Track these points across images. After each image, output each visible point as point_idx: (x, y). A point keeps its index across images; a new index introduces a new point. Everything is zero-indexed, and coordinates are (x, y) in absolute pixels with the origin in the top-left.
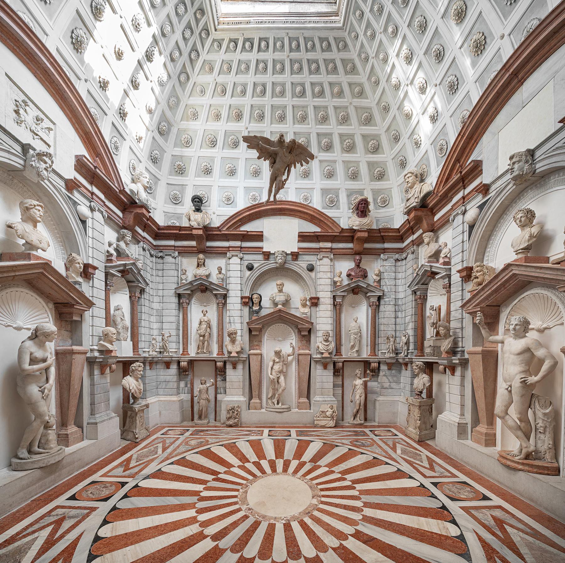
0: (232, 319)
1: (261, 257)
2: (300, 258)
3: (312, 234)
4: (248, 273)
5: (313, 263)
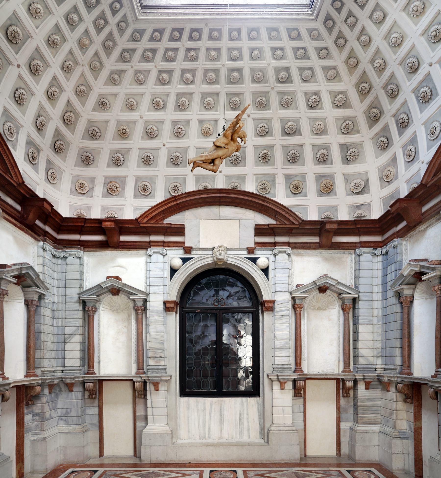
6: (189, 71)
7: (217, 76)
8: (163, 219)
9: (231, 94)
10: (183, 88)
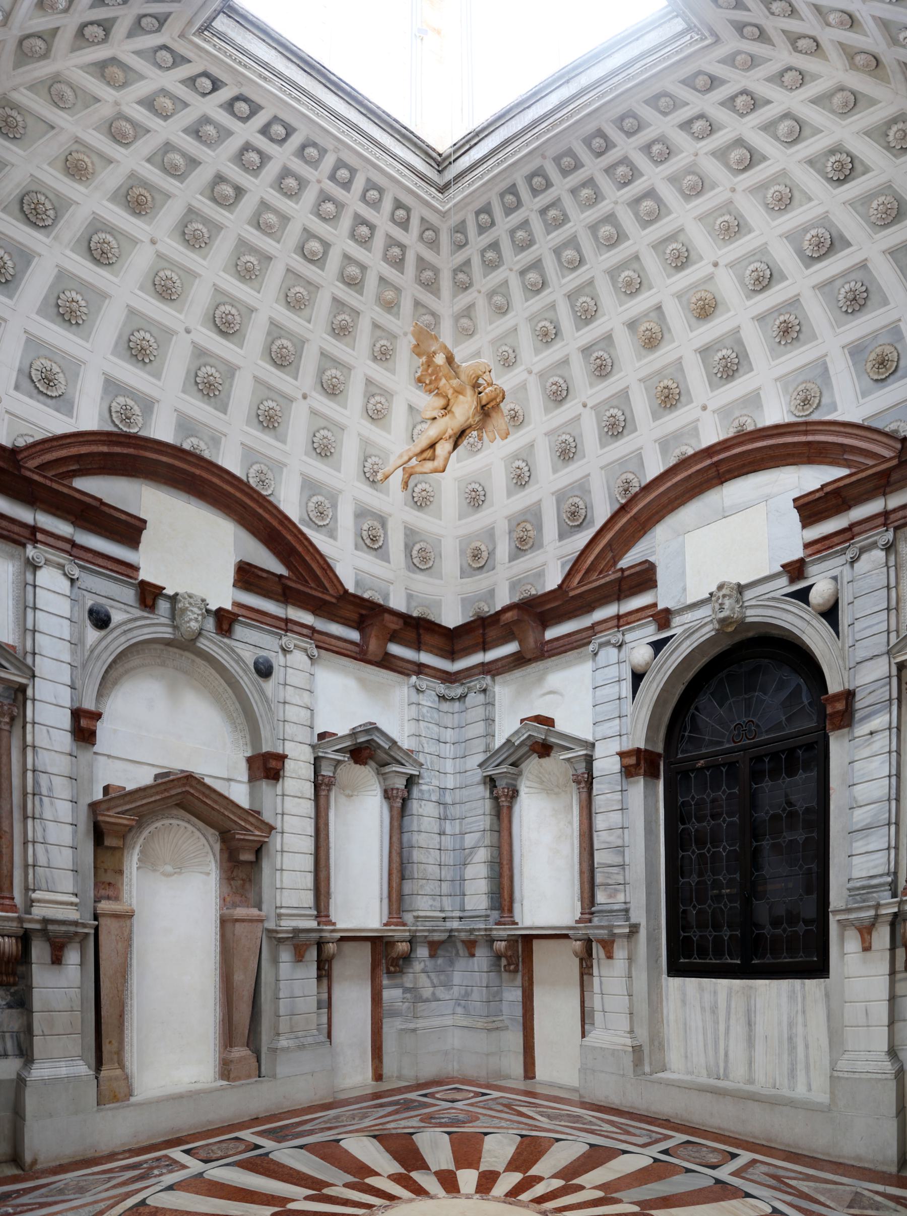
0: (43, 780)
1: (129, 595)
2: (240, 631)
4: (92, 635)
5: (271, 656)
6: (566, 245)
7: (617, 225)
8: (615, 563)
9: (661, 242)
10: (573, 280)
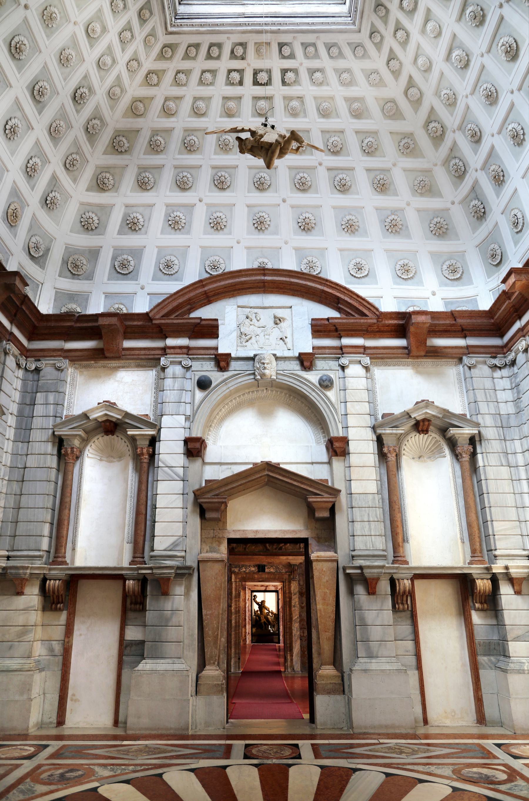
3: (327, 322)
